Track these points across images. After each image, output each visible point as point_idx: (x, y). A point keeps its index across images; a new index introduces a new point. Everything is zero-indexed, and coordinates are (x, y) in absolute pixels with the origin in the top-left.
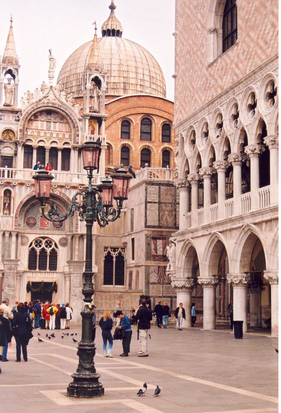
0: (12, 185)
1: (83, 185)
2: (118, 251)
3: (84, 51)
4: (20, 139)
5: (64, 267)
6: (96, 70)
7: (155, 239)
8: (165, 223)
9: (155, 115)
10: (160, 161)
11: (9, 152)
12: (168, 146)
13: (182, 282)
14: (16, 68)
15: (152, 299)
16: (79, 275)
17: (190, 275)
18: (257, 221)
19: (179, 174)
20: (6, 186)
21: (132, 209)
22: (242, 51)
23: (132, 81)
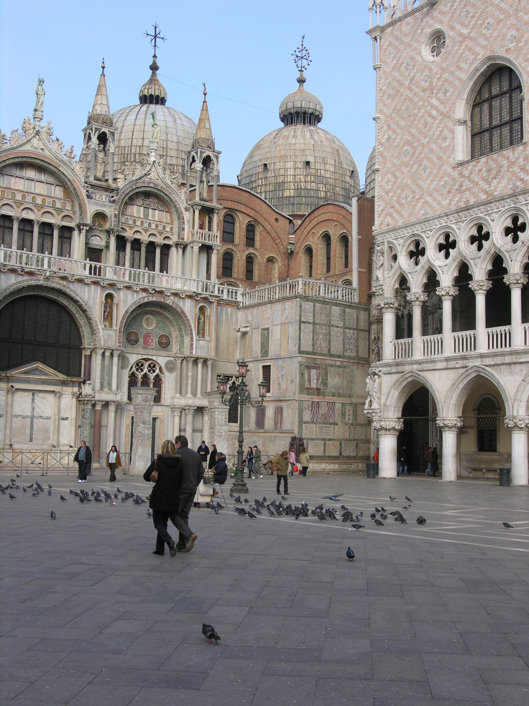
2: (232, 381)
3: (129, 118)
6: (208, 147)
7: (309, 368)
9: (240, 211)
10: (244, 269)
12: (253, 252)
13: (392, 423)
14: (112, 130)
15: (305, 442)
19: (385, 292)
20: (108, 289)
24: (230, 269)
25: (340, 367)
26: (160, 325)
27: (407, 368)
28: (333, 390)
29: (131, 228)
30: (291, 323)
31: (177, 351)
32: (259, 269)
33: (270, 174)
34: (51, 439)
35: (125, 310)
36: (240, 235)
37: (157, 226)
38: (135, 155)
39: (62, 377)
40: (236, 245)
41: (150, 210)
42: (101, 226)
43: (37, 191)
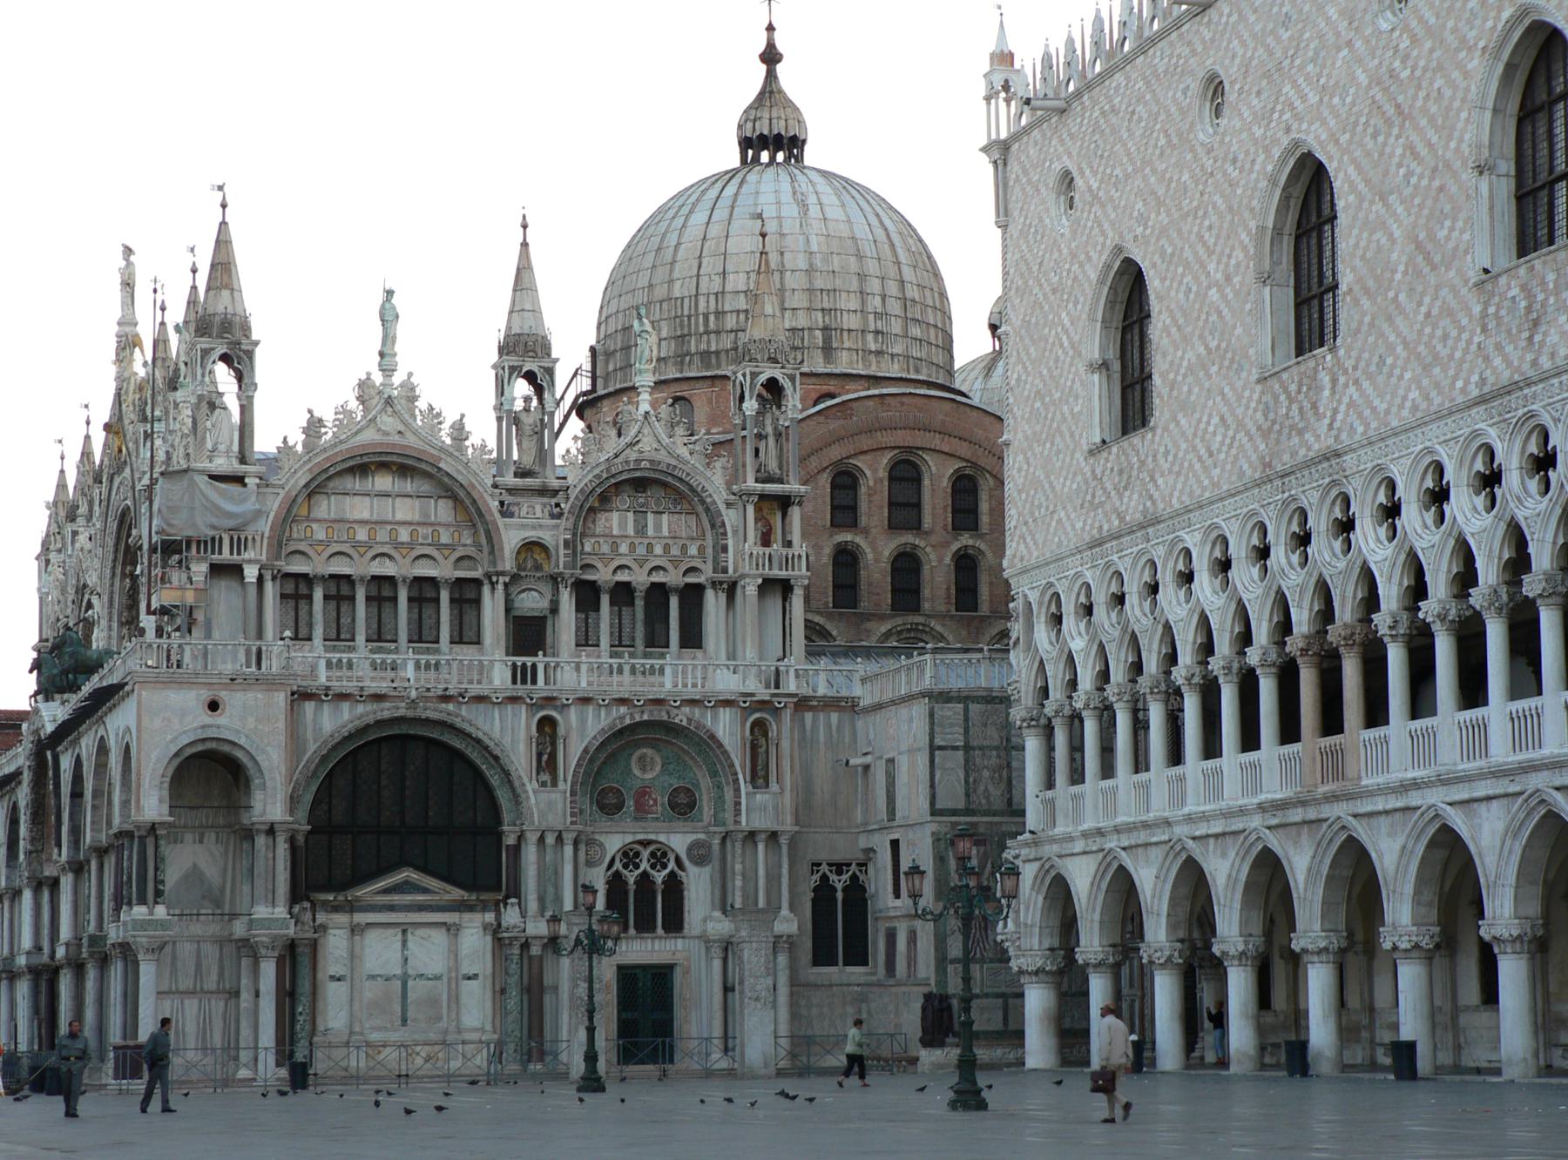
0: (558, 703)
1: (752, 695)
3: (693, 220)
4: (565, 568)
5: (705, 920)
8: (984, 801)
10: (948, 589)
11: (534, 605)
12: (971, 542)
14: (546, 365)
17: (1056, 944)
18: (1198, 833)
20: (542, 707)
21: (891, 761)
22: (1162, 449)
23: (852, 322)
24: (916, 591)
26: (672, 766)
30: (919, 750)
32: (991, 583)
34: (445, 1018)
35: (581, 749)
36: (934, 508)
37: (666, 548)
38: (706, 316)
39: (457, 894)
40: (926, 533)
41: (650, 517)
43: (399, 516)
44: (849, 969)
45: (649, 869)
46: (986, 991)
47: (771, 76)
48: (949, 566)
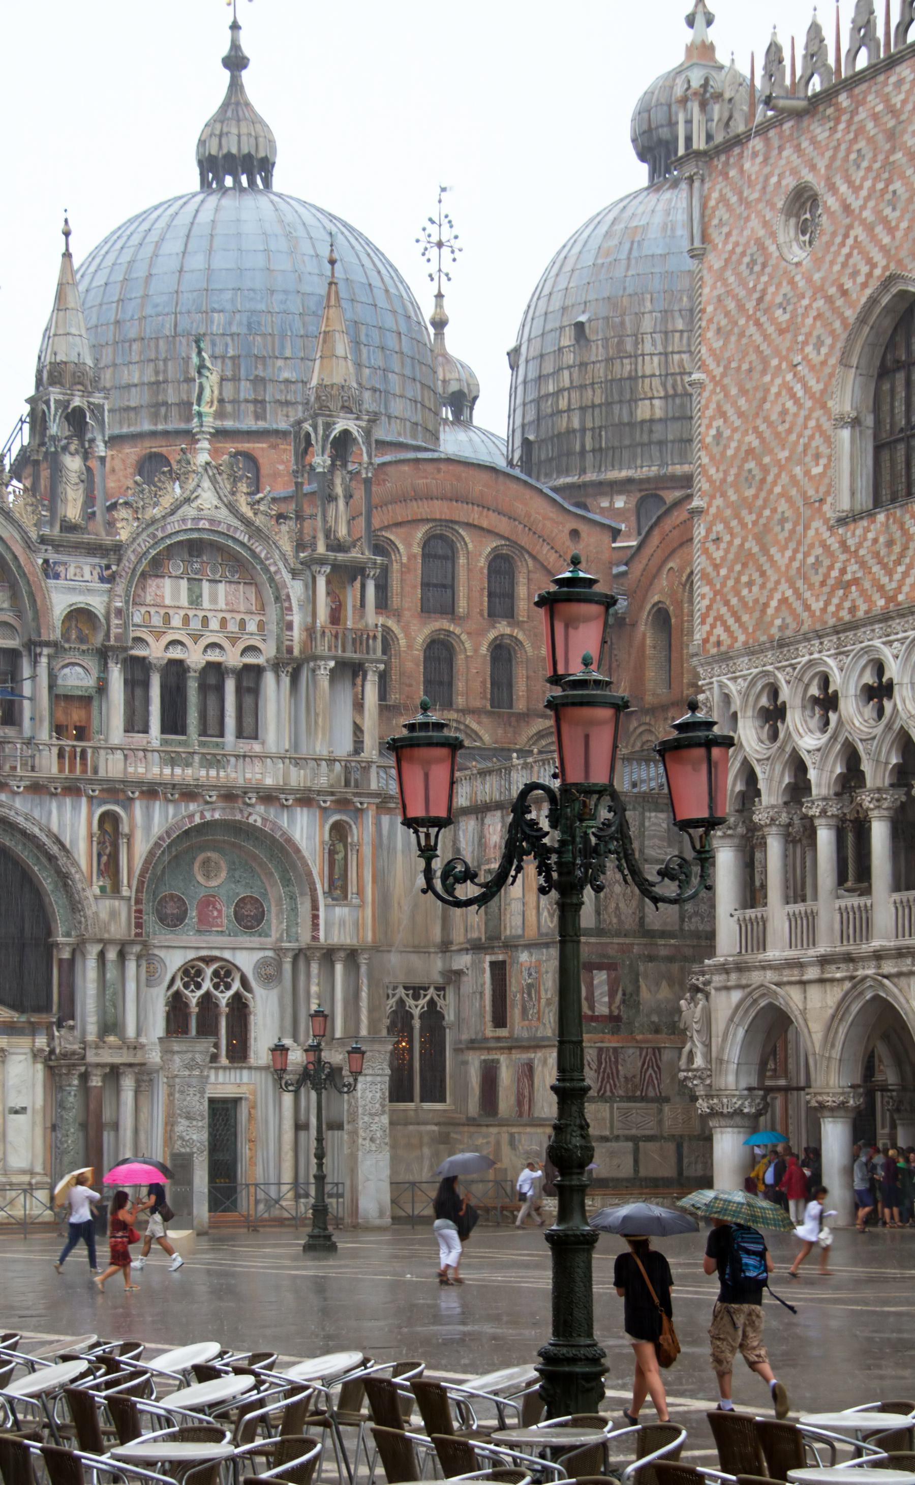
2: (428, 998)
10: (484, 683)
12: (508, 631)
13: (734, 1100)
16: (379, 1079)
25: (670, 959)
26: (237, 874)
27: (756, 977)
28: (655, 1018)
29: (158, 635)
31: (282, 935)
32: (528, 678)
33: (597, 352)
36: (470, 589)
37: (223, 622)
40: (460, 618)
41: (206, 585)
42: (82, 639)
44: (427, 1106)
45: (212, 989)
46: (616, 1132)
47: (235, 86)
48: (485, 656)
